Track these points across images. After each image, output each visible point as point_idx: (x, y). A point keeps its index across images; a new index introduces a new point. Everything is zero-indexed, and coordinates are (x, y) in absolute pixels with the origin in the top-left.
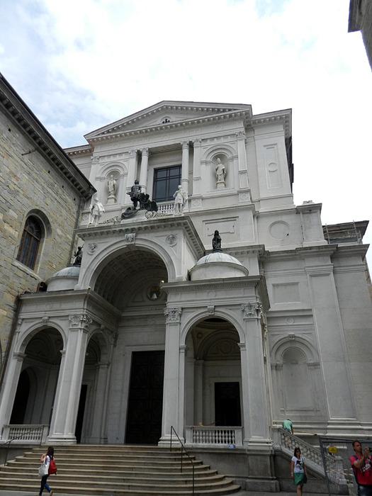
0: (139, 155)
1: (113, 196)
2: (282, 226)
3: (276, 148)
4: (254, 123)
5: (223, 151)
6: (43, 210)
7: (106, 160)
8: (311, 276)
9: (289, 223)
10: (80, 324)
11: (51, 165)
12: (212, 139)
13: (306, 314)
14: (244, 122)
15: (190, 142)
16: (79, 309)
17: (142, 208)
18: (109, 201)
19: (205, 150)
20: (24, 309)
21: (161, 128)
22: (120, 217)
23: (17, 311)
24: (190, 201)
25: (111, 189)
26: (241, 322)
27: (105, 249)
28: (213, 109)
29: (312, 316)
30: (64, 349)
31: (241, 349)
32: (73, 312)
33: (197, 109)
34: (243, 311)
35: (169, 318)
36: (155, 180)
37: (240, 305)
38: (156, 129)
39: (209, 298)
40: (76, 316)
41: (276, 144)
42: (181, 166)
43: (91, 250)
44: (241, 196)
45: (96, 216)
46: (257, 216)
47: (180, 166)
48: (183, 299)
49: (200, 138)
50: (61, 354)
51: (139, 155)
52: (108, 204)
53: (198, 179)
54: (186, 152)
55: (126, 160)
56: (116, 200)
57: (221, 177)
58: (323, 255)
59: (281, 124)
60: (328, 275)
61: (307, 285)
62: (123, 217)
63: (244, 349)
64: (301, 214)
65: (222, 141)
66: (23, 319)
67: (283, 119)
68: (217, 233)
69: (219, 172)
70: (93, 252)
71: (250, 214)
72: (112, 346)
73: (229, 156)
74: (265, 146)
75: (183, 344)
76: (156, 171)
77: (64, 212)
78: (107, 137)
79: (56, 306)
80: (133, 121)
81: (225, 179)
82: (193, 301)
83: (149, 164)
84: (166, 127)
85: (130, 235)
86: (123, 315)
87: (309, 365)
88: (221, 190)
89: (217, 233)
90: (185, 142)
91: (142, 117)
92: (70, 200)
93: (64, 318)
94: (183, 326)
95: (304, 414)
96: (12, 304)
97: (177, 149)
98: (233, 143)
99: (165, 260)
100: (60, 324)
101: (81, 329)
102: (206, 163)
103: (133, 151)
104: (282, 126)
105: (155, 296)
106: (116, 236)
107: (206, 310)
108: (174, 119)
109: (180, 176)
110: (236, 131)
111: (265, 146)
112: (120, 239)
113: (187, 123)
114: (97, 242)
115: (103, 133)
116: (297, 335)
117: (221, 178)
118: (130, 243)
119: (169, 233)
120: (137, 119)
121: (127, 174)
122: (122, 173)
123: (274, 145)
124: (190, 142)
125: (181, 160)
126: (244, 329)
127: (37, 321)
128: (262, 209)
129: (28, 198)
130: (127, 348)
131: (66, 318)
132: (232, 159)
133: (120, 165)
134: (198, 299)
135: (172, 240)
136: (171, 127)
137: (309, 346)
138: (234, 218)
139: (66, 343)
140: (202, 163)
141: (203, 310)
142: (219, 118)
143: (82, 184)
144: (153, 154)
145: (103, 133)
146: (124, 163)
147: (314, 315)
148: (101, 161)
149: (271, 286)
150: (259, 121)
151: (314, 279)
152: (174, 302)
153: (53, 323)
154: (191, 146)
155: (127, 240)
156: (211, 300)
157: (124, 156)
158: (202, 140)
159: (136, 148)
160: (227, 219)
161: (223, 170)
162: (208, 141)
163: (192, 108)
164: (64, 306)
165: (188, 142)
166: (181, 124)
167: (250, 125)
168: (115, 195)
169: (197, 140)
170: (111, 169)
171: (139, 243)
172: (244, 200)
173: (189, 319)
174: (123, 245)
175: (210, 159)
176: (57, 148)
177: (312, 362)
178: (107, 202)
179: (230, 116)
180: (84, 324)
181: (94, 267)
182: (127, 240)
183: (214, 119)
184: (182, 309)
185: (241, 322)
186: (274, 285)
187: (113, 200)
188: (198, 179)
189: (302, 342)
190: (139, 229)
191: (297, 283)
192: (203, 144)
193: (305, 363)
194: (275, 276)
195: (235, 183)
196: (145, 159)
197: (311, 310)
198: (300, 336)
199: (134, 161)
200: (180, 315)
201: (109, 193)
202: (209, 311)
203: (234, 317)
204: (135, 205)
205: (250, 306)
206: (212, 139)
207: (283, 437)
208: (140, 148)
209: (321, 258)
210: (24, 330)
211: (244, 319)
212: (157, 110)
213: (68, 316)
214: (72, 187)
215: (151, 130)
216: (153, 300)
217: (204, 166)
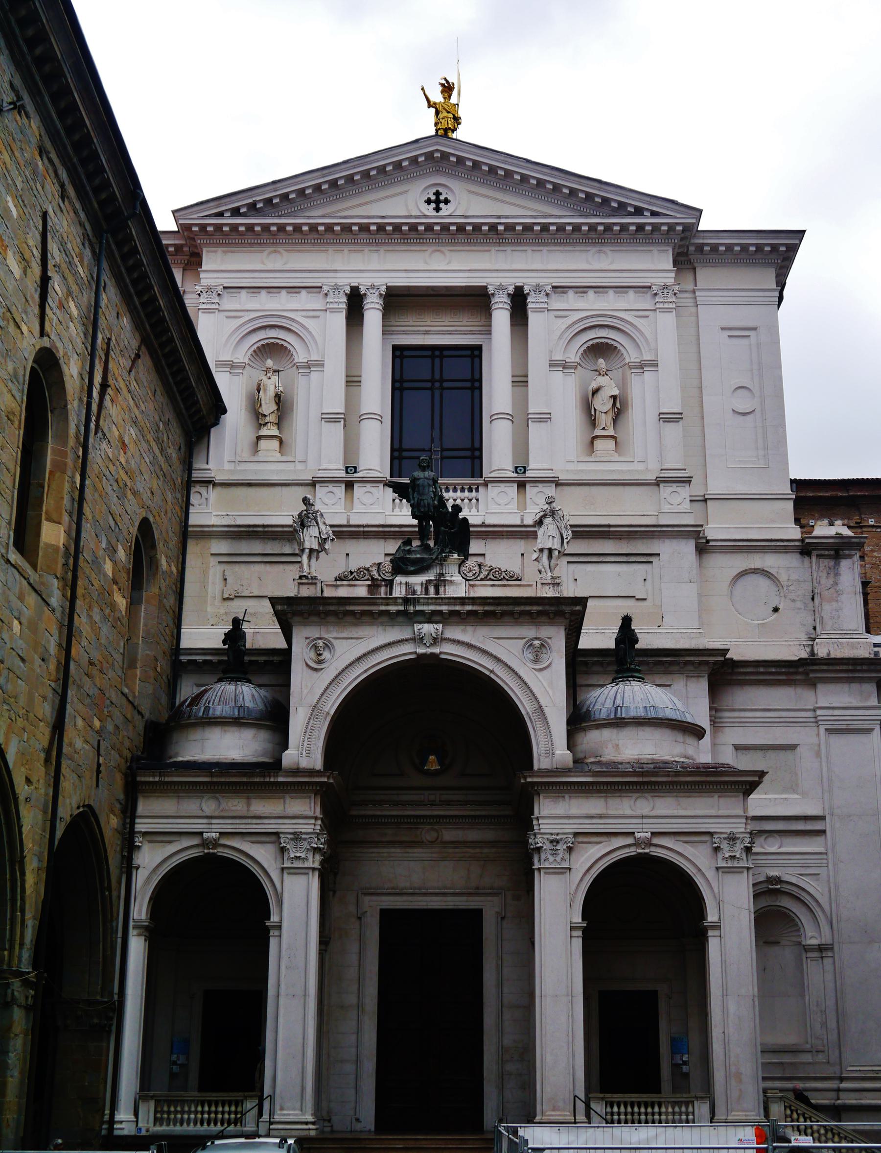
0: (355, 302)
1: (273, 431)
2: (763, 583)
3: (753, 339)
4: (700, 248)
5: (612, 334)
6: (151, 519)
7: (245, 301)
8: (829, 731)
9: (783, 578)
10: (310, 856)
12: (582, 289)
13: (808, 827)
14: (673, 250)
15: (519, 290)
16: (301, 816)
18: (263, 444)
19: (563, 324)
20: (142, 807)
21: (429, 228)
22: (388, 566)
23: (129, 813)
24: (522, 485)
25: (268, 407)
26: (710, 874)
27: (359, 659)
28: (589, 197)
29: (823, 832)
30: (274, 918)
31: (710, 933)
32: (286, 827)
33: (541, 183)
34: (717, 849)
35: (543, 856)
36: (400, 386)
37: (711, 834)
38: (413, 227)
39: (639, 812)
40: (297, 837)
41: (754, 329)
42: (479, 348)
43: (313, 655)
44: (666, 491)
45: (312, 550)
46: (704, 548)
47: (474, 353)
48: (574, 811)
49: (548, 280)
50: (267, 930)
52: (261, 456)
53: (545, 418)
54: (501, 318)
55: (313, 314)
56: (281, 442)
57: (604, 418)
58: (861, 680)
59: (768, 265)
60: (868, 731)
61: (818, 754)
62: (401, 564)
63: (716, 933)
64: (814, 559)
65: (609, 303)
66: (145, 834)
67: (775, 252)
68: (627, 621)
69: (602, 404)
70: (320, 662)
71: (688, 547)
72: (331, 893)
73: (631, 355)
74: (723, 329)
75: (578, 918)
76: (400, 353)
77: (169, 497)
79: (237, 805)
80: (333, 184)
81: (615, 421)
82: (600, 817)
83: (386, 332)
84: (445, 227)
85: (427, 629)
86: (354, 813)
87: (807, 949)
88: (607, 464)
89: (627, 621)
90: (501, 287)
91: (366, 174)
92: (173, 452)
93: (254, 839)
94: (576, 875)
95: (787, 1059)
96: (122, 797)
97: (476, 300)
98: (642, 313)
99: (525, 706)
100: (251, 853)
101: (314, 869)
102: (565, 366)
103: (336, 287)
104: (773, 270)
105: (432, 762)
106: (382, 624)
107: (630, 841)
108: (468, 203)
109: (474, 385)
110: (657, 280)
111: (723, 329)
112: (406, 633)
113: (510, 227)
114: (330, 633)
115: (236, 212)
116: (786, 878)
117: (604, 420)
118: (422, 650)
119: (529, 632)
120: (350, 179)
121: (320, 364)
122: (301, 356)
123: (754, 329)
124: (519, 290)
125: (489, 333)
126: (715, 885)
127: (186, 842)
128: (717, 529)
129: (135, 493)
130: (367, 899)
131: (273, 838)
132: (642, 366)
134: (611, 812)
135: (538, 650)
136: (461, 228)
137: (812, 904)
138: (648, 558)
139: (280, 903)
140: (553, 364)
141: (630, 841)
142: (608, 228)
143: (201, 396)
144: (398, 301)
145: (236, 212)
146: (310, 323)
147: (828, 833)
148: (229, 302)
149: (731, 748)
150: (715, 248)
151: (835, 739)
152: (553, 816)
153: (225, 846)
154: (519, 302)
155: (419, 640)
156: (643, 817)
157: (304, 300)
158: (554, 287)
159: (347, 281)
160: (628, 558)
161: (614, 397)
162: (571, 293)
163: (525, 178)
164: (260, 807)
165: (511, 290)
166: (493, 227)
167: (686, 254)
168: (278, 425)
169: (538, 289)
170: (262, 335)
171: (448, 651)
172: (674, 507)
173: (590, 859)
174: (407, 651)
175: (573, 355)
177: (814, 942)
178: (255, 449)
179: (640, 227)
180: (318, 858)
181: (332, 705)
182: (419, 640)
183: (593, 227)
184: (576, 834)
185: (710, 874)
186: (737, 748)
187: (275, 444)
188: (545, 418)
189: (797, 895)
190: (452, 613)
191: (793, 747)
192: (558, 303)
193: (800, 943)
194: (742, 724)
195: (647, 446)
196: (373, 317)
197: (822, 818)
198: (793, 880)
199: (339, 321)
200: (570, 849)
201: (258, 417)
202: (637, 844)
203: (696, 860)
204: (423, 533)
205: (732, 839)
206: (582, 289)
207: (788, 1112)
208: (363, 281)
209: (855, 686)
210: (151, 862)
211: (717, 869)
212: (414, 160)
213: (277, 834)
215: (397, 227)
216: (429, 773)
217: (558, 376)
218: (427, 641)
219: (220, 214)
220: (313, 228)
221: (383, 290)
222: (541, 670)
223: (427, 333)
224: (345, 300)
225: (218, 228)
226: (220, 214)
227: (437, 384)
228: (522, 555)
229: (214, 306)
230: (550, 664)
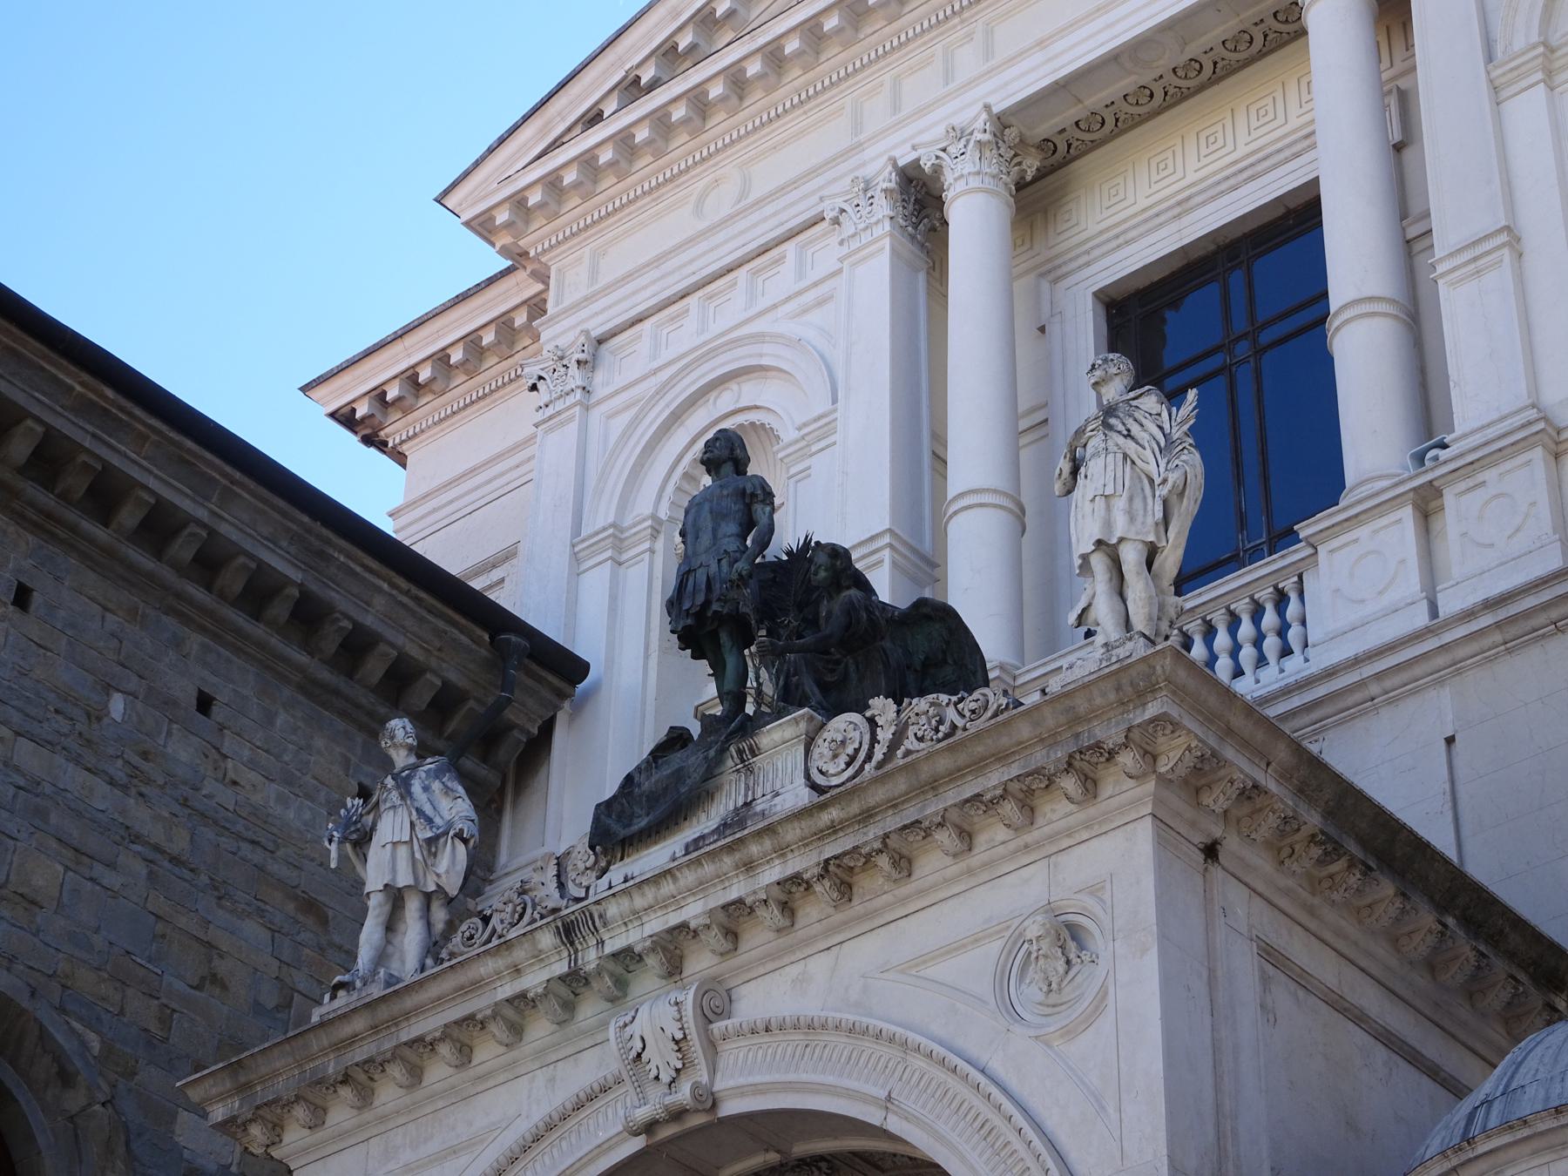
11: (43, 525)
17: (789, 698)
24: (1427, 503)
45: (396, 898)
51: (920, 198)
78: (624, 140)
85: (657, 1013)
115: (593, 118)
133: (769, 355)
145: (593, 118)
171: (749, 1081)
176: (77, 381)
214: (310, 688)
218: (661, 1058)
219: (556, 144)
220: (774, 56)
221: (981, 130)
222: (1069, 1033)
223: (1184, 206)
224: (884, 207)
225: (552, 182)
226: (556, 144)
227: (1243, 349)
228: (1450, 741)
229: (570, 400)
230: (1103, 994)
